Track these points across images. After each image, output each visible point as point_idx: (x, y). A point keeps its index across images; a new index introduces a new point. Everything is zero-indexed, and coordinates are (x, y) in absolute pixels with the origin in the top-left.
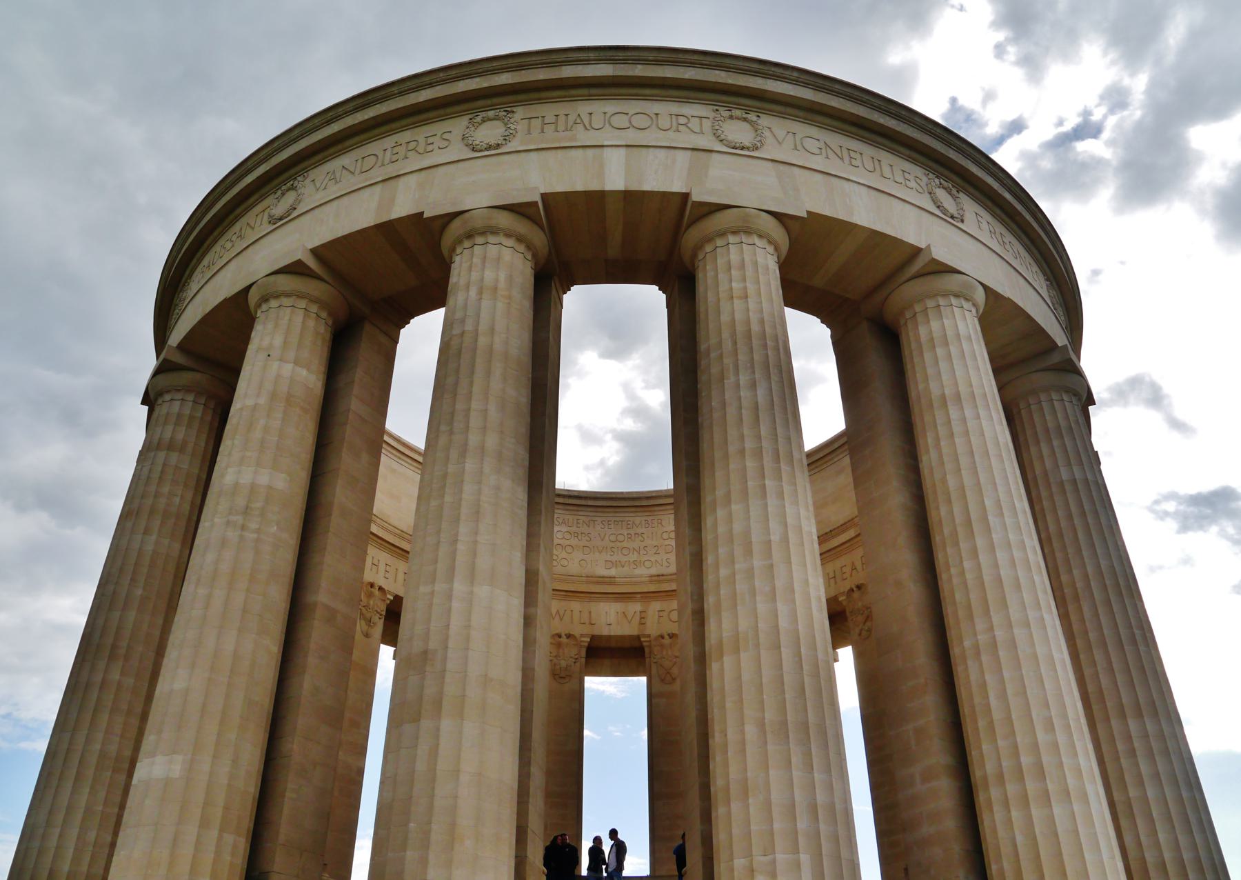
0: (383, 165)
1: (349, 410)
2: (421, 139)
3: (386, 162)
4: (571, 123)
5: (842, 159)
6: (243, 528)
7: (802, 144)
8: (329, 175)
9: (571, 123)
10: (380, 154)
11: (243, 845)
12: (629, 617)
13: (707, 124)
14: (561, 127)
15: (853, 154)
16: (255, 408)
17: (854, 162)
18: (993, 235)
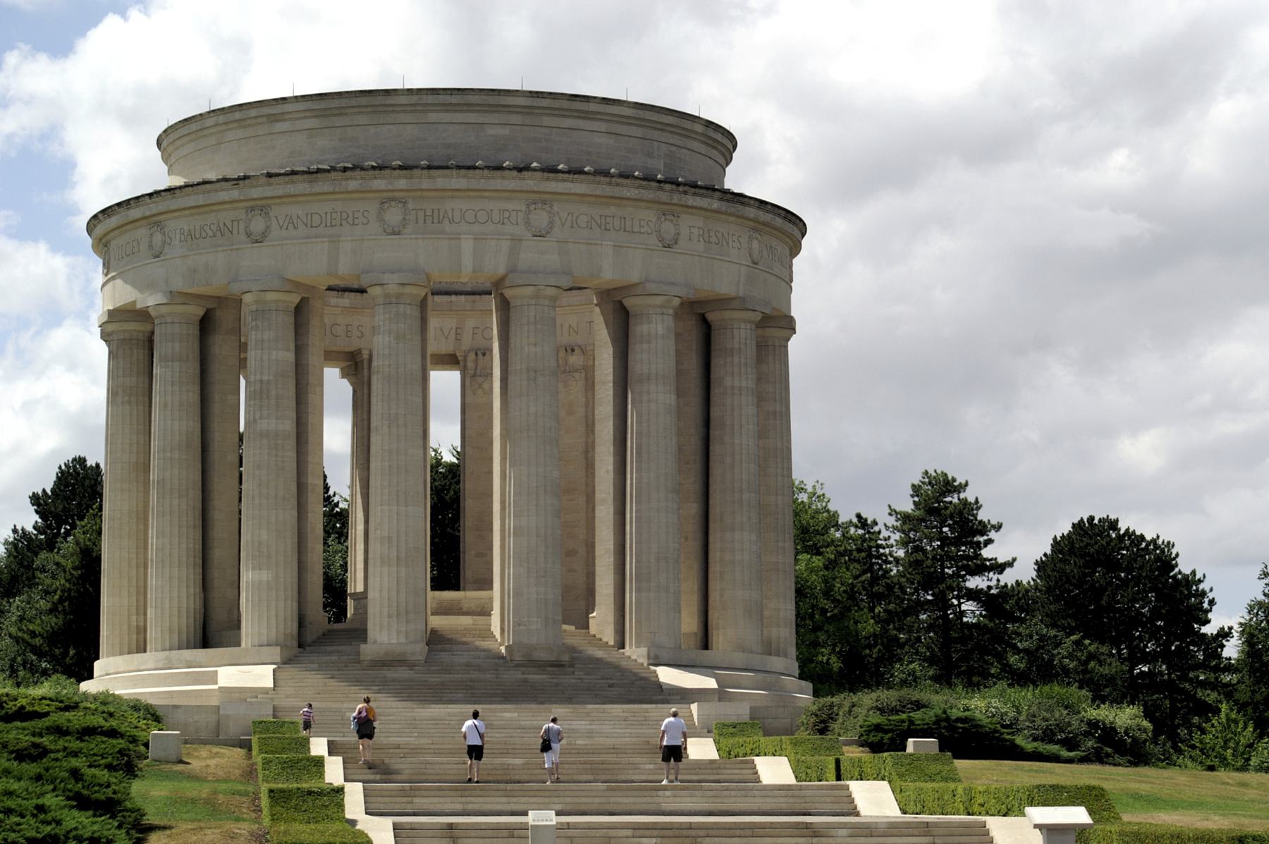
0: (326, 226)
1: (308, 364)
2: (351, 215)
3: (329, 224)
4: (441, 217)
5: (600, 227)
6: (276, 456)
7: (577, 217)
8: (288, 218)
9: (441, 217)
10: (323, 216)
11: (295, 605)
12: (446, 334)
13: (521, 215)
14: (436, 221)
15: (609, 220)
16: (268, 382)
17: (608, 228)
18: (701, 239)
